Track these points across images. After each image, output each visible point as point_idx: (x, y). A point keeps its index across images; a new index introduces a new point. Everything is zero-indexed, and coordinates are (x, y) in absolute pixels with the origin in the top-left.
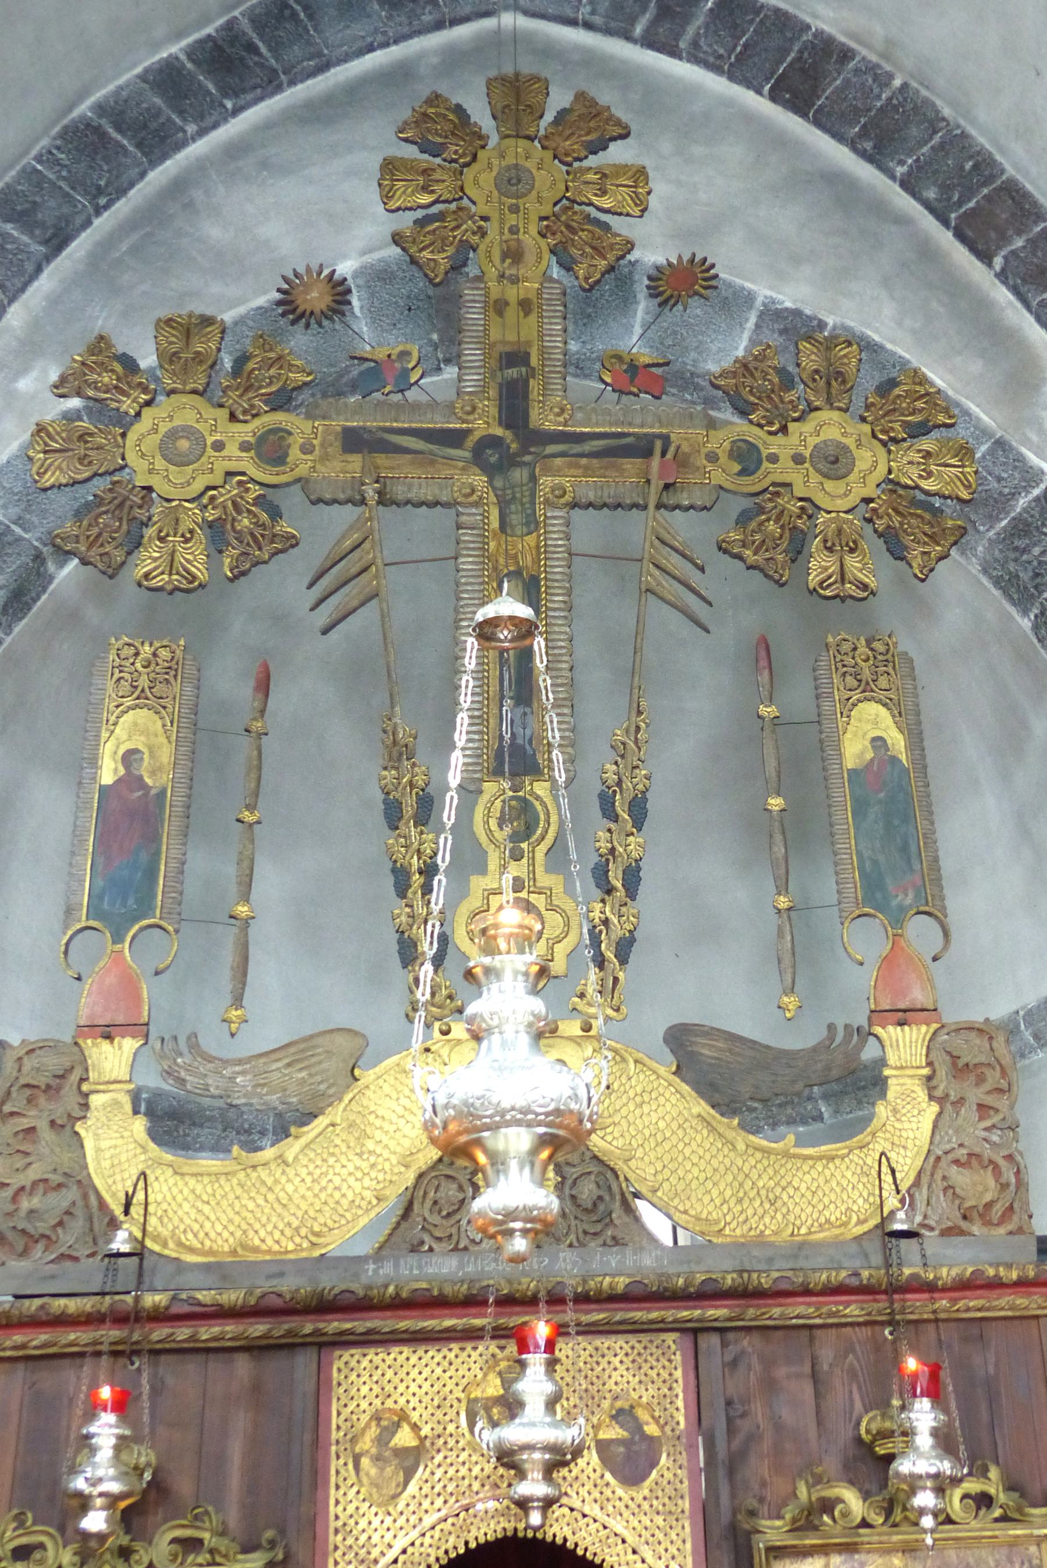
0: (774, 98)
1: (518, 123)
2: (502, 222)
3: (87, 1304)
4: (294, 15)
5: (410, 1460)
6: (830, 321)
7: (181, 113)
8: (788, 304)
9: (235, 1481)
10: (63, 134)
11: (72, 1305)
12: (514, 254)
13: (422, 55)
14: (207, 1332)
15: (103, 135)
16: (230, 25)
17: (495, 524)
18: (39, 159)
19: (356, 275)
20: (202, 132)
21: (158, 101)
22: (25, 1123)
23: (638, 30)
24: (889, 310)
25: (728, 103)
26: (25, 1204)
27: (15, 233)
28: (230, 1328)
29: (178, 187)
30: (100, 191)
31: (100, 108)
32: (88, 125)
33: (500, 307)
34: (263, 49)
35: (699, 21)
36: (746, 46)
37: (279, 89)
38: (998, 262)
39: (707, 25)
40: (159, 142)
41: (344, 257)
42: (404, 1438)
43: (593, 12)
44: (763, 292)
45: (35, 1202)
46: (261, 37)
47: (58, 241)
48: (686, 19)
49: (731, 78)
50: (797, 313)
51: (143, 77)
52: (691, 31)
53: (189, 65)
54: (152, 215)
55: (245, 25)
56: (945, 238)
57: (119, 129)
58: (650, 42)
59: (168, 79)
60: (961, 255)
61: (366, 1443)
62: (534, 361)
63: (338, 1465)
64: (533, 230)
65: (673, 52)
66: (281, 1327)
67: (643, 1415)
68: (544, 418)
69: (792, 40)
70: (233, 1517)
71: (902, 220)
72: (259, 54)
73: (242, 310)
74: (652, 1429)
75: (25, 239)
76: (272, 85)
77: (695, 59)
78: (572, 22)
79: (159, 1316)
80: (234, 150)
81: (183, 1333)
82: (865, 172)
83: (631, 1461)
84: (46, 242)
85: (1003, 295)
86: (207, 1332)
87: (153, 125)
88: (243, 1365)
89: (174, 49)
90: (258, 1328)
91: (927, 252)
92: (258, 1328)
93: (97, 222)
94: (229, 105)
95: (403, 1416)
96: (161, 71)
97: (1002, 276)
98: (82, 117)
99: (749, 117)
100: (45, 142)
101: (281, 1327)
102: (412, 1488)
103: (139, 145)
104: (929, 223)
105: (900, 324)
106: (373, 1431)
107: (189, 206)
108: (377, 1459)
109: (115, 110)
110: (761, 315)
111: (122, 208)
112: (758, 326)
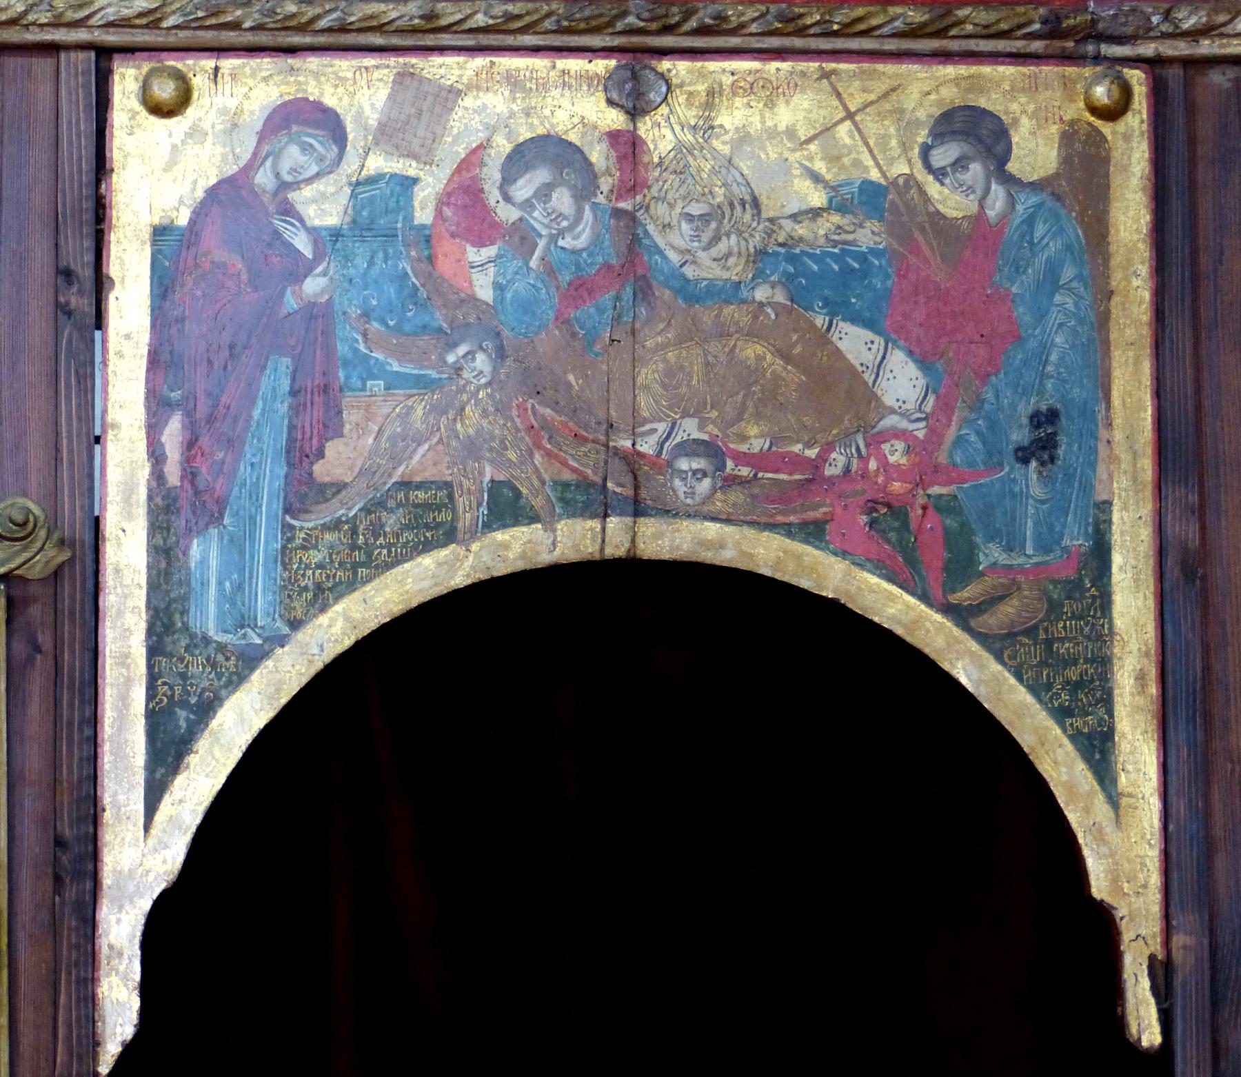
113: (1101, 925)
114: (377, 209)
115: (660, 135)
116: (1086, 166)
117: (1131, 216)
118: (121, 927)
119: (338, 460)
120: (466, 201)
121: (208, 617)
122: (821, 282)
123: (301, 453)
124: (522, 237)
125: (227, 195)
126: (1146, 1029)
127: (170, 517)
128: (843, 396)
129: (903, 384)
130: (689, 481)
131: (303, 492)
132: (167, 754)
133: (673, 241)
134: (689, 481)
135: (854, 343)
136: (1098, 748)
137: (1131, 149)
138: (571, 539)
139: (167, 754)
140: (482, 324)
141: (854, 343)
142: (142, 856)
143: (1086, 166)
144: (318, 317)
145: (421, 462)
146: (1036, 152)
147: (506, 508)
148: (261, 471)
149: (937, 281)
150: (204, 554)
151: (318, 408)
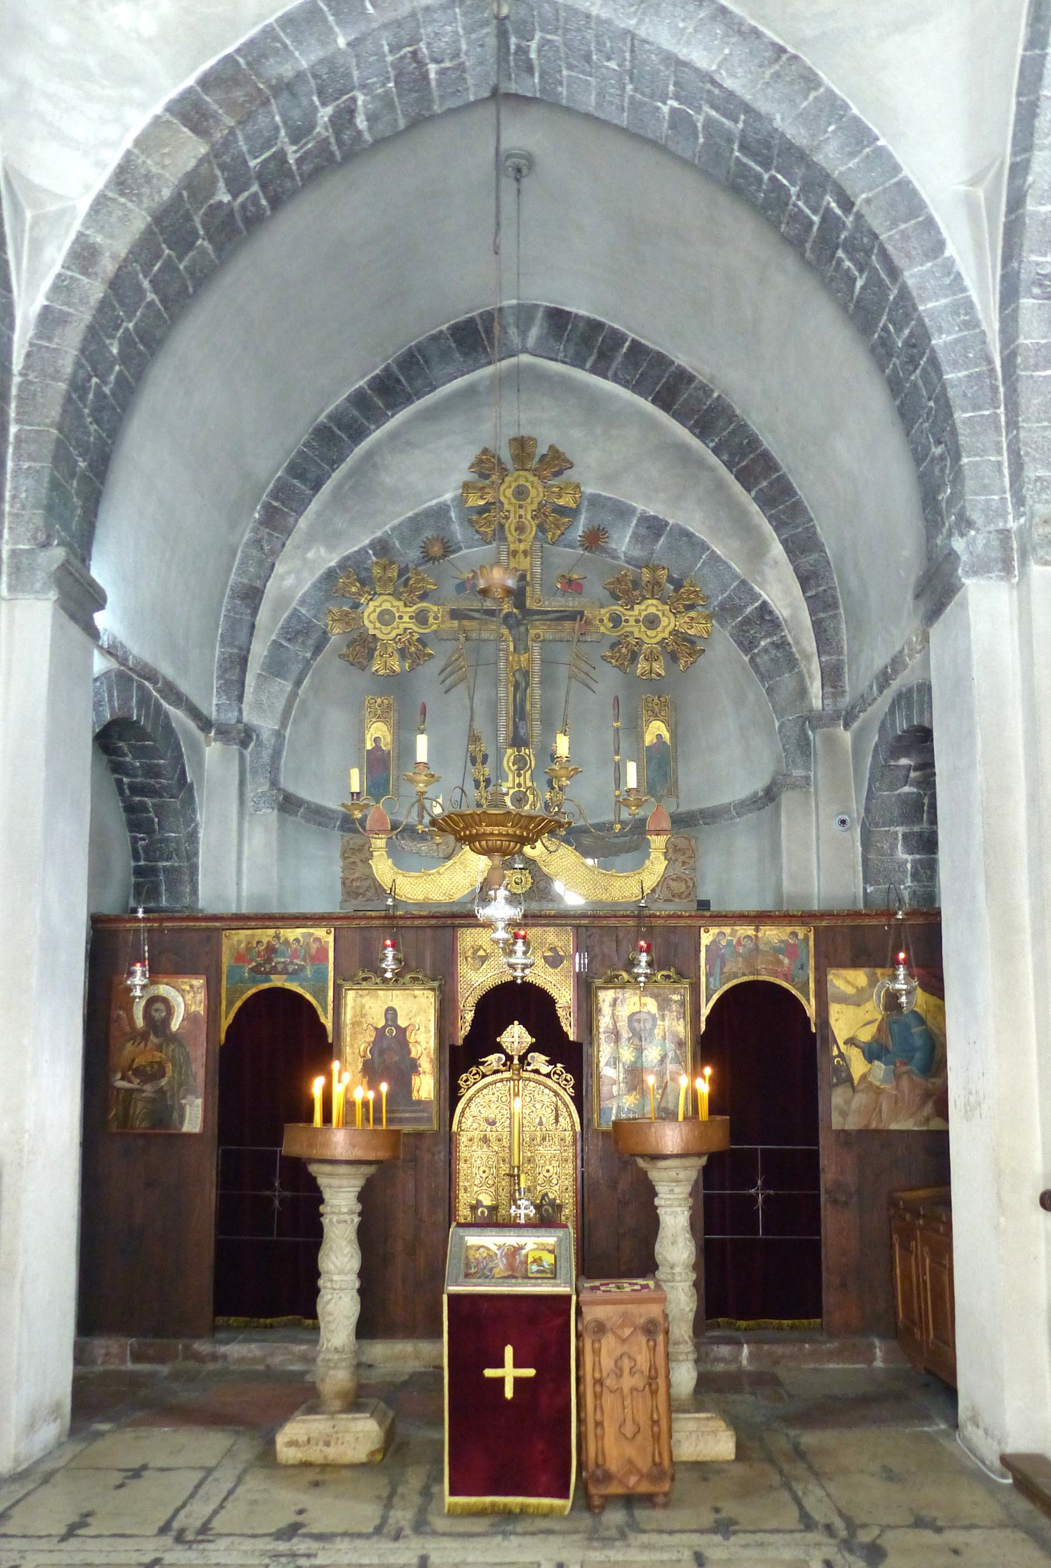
0: (653, 402)
1: (523, 463)
2: (515, 512)
3: (377, 914)
4: (418, 362)
5: (483, 959)
6: (671, 521)
7: (368, 419)
8: (652, 513)
9: (428, 963)
10: (313, 433)
11: (373, 914)
12: (520, 528)
13: (482, 378)
14: (417, 922)
15: (333, 432)
16: (387, 369)
17: (512, 649)
18: (304, 445)
19: (453, 500)
20: (378, 428)
21: (356, 413)
22: (352, 860)
23: (588, 365)
24: (698, 516)
25: (630, 404)
26: (355, 884)
27: (298, 484)
28: (424, 922)
29: (369, 455)
30: (334, 462)
31: (330, 417)
32: (325, 427)
33: (515, 553)
34: (404, 381)
35: (619, 359)
36: (642, 374)
37: (412, 402)
38: (753, 493)
39: (622, 363)
40: (358, 434)
41: (447, 491)
42: (481, 953)
43: (565, 356)
44: (640, 507)
45: (358, 884)
46: (403, 374)
47: (317, 487)
48: (612, 359)
49: (633, 391)
50: (655, 518)
51: (348, 399)
52: (614, 366)
53: (369, 392)
54: (356, 472)
55: (395, 368)
56: (730, 478)
57: (339, 429)
58: (594, 371)
59: (359, 399)
60: (737, 488)
61: (469, 953)
62: (528, 579)
63: (460, 960)
64: (529, 517)
65: (605, 377)
66: (440, 922)
67: (559, 949)
68: (529, 604)
69: (664, 371)
70: (428, 972)
71: (711, 469)
72: (402, 385)
73: (402, 518)
74: (562, 953)
75: (303, 487)
76: (409, 400)
77: (616, 379)
78: (556, 360)
79: (401, 917)
80: (394, 436)
81: (409, 923)
82: (694, 442)
83: (554, 961)
84: (312, 489)
85: (755, 508)
86: (417, 922)
87: (356, 426)
88: (429, 931)
89: (361, 383)
90: (433, 922)
91: (720, 485)
92: (433, 922)
93: (333, 475)
94: (390, 414)
95: (481, 947)
96: (356, 396)
97: (755, 499)
98: (322, 423)
99: (641, 414)
100: (306, 436)
101: (440, 922)
102: (484, 966)
103: (349, 438)
104: (723, 470)
105: (703, 523)
106: (471, 951)
107: (374, 466)
108: (473, 958)
109: (336, 417)
110: (639, 520)
111: (344, 468)
112: (637, 525)
113: (808, 1020)
114: (729, 943)
115: (760, 935)
116: (806, 938)
117: (811, 943)
118: (703, 1019)
119: (725, 970)
120: (739, 942)
121: (712, 986)
122: (777, 950)
123: (722, 969)
124: (745, 946)
125: (713, 942)
126: (814, 1030)
127: (708, 976)
128: (780, 963)
129: (786, 961)
130: (763, 971)
131: (722, 973)
132: (708, 1001)
133: (761, 946)
134: (763, 971)
135: (781, 957)
136: (808, 1000)
137: (812, 935)
138: (751, 978)
139: (708, 1001)
140: (740, 955)
141: (781, 957)
142: (705, 1011)
143: (806, 938)
144: (723, 954)
145: (735, 970)
146: (801, 936)
147: (744, 975)
148: (717, 970)
149: (789, 949)
150: (711, 979)
151: (723, 964)
